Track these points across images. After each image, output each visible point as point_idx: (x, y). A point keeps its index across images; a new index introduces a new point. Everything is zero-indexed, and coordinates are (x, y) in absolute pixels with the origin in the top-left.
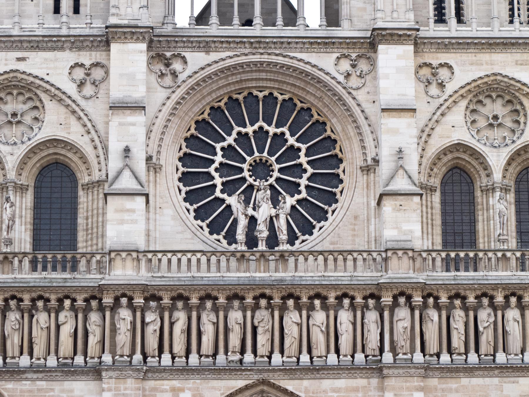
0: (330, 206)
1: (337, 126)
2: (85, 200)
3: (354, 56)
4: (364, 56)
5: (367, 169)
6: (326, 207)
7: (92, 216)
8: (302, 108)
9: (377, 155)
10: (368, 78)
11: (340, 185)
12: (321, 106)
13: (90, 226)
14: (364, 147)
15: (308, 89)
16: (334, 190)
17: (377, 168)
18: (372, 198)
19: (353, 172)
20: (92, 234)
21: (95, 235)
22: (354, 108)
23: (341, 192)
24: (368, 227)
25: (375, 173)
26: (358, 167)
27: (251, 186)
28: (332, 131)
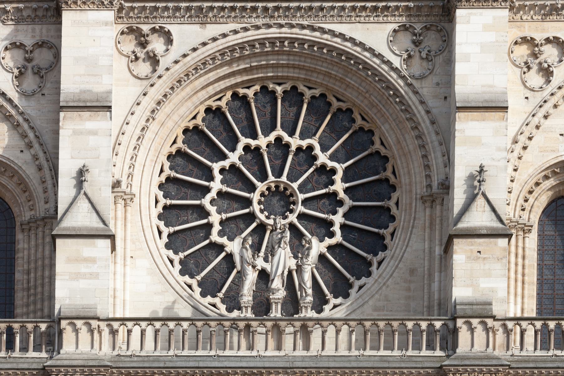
0: (376, 254)
1: (390, 135)
2: (26, 246)
3: (418, 27)
4: (434, 28)
5: (431, 199)
6: (369, 257)
7: (36, 269)
8: (339, 110)
9: (447, 178)
10: (439, 60)
11: (390, 224)
12: (367, 106)
13: (32, 283)
14: (427, 167)
15: (349, 80)
16: (382, 231)
17: (446, 197)
18: (437, 242)
19: (411, 204)
20: (35, 295)
21: (39, 296)
22: (416, 108)
23: (392, 234)
24: (430, 286)
25: (442, 204)
26: (418, 196)
27: (262, 227)
28: (382, 144)
